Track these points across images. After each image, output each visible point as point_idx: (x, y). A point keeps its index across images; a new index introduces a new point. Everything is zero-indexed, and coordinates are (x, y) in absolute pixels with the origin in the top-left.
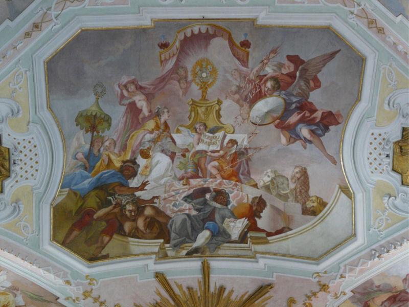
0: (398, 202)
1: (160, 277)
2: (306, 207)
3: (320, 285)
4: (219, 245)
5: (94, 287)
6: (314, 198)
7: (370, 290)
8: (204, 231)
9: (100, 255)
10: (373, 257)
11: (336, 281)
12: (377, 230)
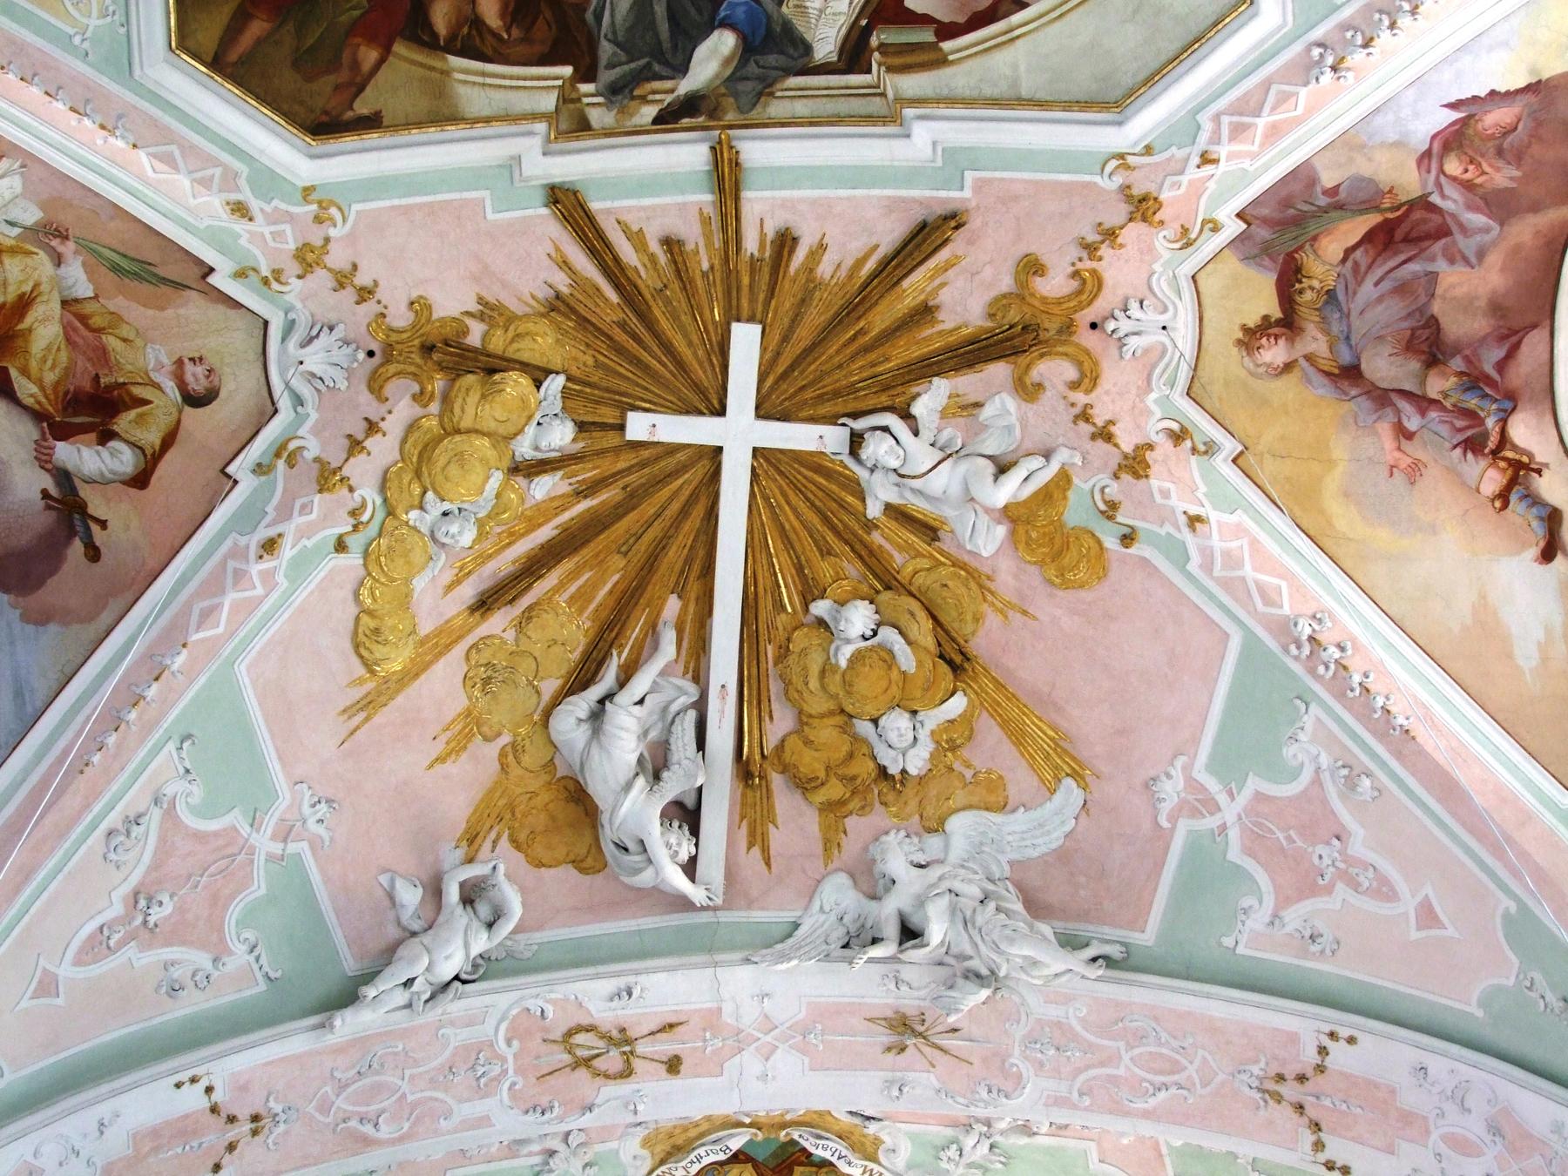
1: (566, 203)
3: (1129, 198)
4: (770, 85)
5: (332, 232)
7: (1306, 208)
8: (716, 33)
9: (350, 114)
10: (1316, 71)
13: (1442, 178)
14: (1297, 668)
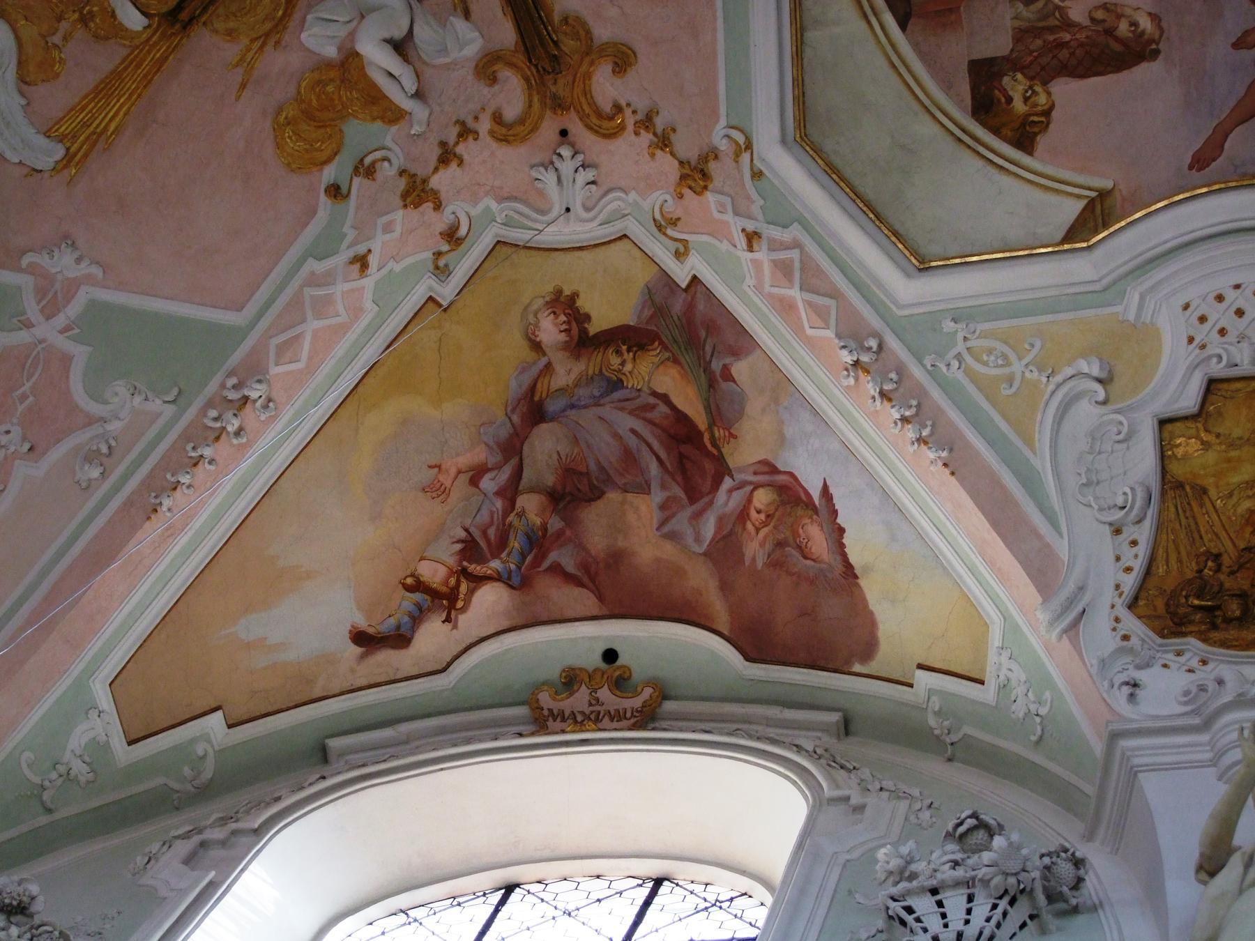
0: (1086, 413)
2: (1001, 75)
3: (704, 159)
6: (1042, 99)
7: (708, 349)
10: (853, 345)
11: (728, 217)
12: (961, 347)
13: (749, 488)
14: (212, 387)
